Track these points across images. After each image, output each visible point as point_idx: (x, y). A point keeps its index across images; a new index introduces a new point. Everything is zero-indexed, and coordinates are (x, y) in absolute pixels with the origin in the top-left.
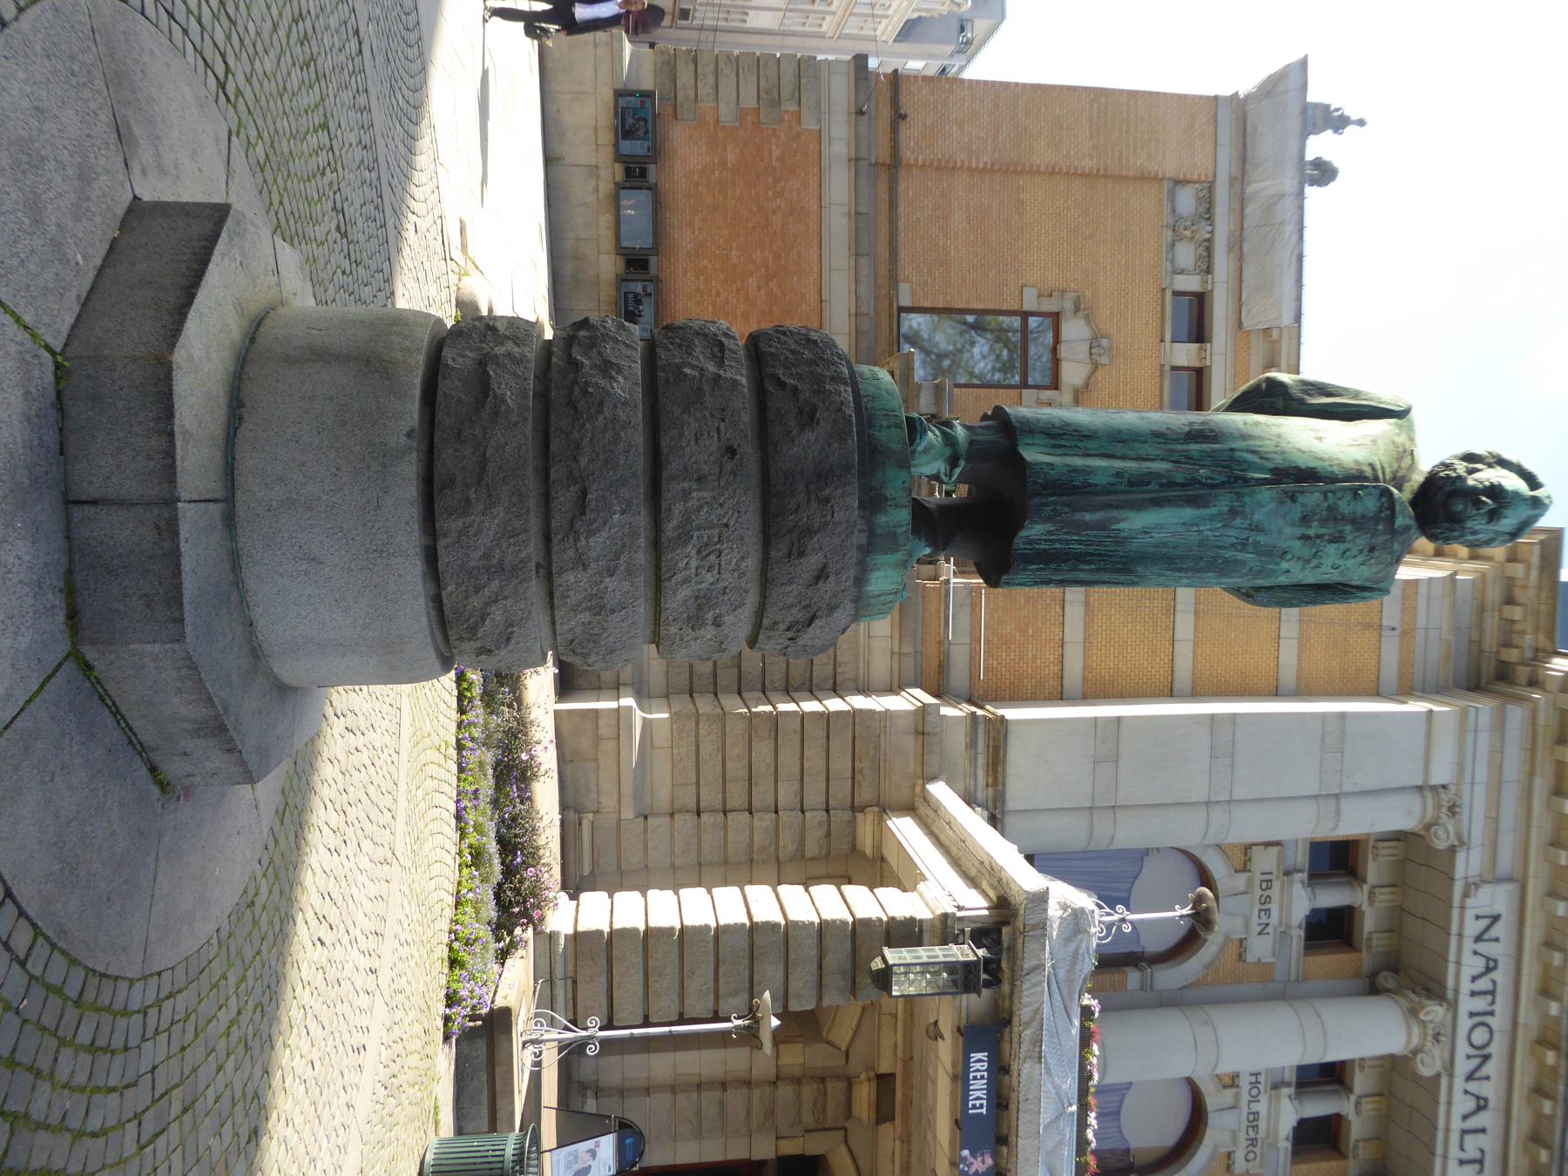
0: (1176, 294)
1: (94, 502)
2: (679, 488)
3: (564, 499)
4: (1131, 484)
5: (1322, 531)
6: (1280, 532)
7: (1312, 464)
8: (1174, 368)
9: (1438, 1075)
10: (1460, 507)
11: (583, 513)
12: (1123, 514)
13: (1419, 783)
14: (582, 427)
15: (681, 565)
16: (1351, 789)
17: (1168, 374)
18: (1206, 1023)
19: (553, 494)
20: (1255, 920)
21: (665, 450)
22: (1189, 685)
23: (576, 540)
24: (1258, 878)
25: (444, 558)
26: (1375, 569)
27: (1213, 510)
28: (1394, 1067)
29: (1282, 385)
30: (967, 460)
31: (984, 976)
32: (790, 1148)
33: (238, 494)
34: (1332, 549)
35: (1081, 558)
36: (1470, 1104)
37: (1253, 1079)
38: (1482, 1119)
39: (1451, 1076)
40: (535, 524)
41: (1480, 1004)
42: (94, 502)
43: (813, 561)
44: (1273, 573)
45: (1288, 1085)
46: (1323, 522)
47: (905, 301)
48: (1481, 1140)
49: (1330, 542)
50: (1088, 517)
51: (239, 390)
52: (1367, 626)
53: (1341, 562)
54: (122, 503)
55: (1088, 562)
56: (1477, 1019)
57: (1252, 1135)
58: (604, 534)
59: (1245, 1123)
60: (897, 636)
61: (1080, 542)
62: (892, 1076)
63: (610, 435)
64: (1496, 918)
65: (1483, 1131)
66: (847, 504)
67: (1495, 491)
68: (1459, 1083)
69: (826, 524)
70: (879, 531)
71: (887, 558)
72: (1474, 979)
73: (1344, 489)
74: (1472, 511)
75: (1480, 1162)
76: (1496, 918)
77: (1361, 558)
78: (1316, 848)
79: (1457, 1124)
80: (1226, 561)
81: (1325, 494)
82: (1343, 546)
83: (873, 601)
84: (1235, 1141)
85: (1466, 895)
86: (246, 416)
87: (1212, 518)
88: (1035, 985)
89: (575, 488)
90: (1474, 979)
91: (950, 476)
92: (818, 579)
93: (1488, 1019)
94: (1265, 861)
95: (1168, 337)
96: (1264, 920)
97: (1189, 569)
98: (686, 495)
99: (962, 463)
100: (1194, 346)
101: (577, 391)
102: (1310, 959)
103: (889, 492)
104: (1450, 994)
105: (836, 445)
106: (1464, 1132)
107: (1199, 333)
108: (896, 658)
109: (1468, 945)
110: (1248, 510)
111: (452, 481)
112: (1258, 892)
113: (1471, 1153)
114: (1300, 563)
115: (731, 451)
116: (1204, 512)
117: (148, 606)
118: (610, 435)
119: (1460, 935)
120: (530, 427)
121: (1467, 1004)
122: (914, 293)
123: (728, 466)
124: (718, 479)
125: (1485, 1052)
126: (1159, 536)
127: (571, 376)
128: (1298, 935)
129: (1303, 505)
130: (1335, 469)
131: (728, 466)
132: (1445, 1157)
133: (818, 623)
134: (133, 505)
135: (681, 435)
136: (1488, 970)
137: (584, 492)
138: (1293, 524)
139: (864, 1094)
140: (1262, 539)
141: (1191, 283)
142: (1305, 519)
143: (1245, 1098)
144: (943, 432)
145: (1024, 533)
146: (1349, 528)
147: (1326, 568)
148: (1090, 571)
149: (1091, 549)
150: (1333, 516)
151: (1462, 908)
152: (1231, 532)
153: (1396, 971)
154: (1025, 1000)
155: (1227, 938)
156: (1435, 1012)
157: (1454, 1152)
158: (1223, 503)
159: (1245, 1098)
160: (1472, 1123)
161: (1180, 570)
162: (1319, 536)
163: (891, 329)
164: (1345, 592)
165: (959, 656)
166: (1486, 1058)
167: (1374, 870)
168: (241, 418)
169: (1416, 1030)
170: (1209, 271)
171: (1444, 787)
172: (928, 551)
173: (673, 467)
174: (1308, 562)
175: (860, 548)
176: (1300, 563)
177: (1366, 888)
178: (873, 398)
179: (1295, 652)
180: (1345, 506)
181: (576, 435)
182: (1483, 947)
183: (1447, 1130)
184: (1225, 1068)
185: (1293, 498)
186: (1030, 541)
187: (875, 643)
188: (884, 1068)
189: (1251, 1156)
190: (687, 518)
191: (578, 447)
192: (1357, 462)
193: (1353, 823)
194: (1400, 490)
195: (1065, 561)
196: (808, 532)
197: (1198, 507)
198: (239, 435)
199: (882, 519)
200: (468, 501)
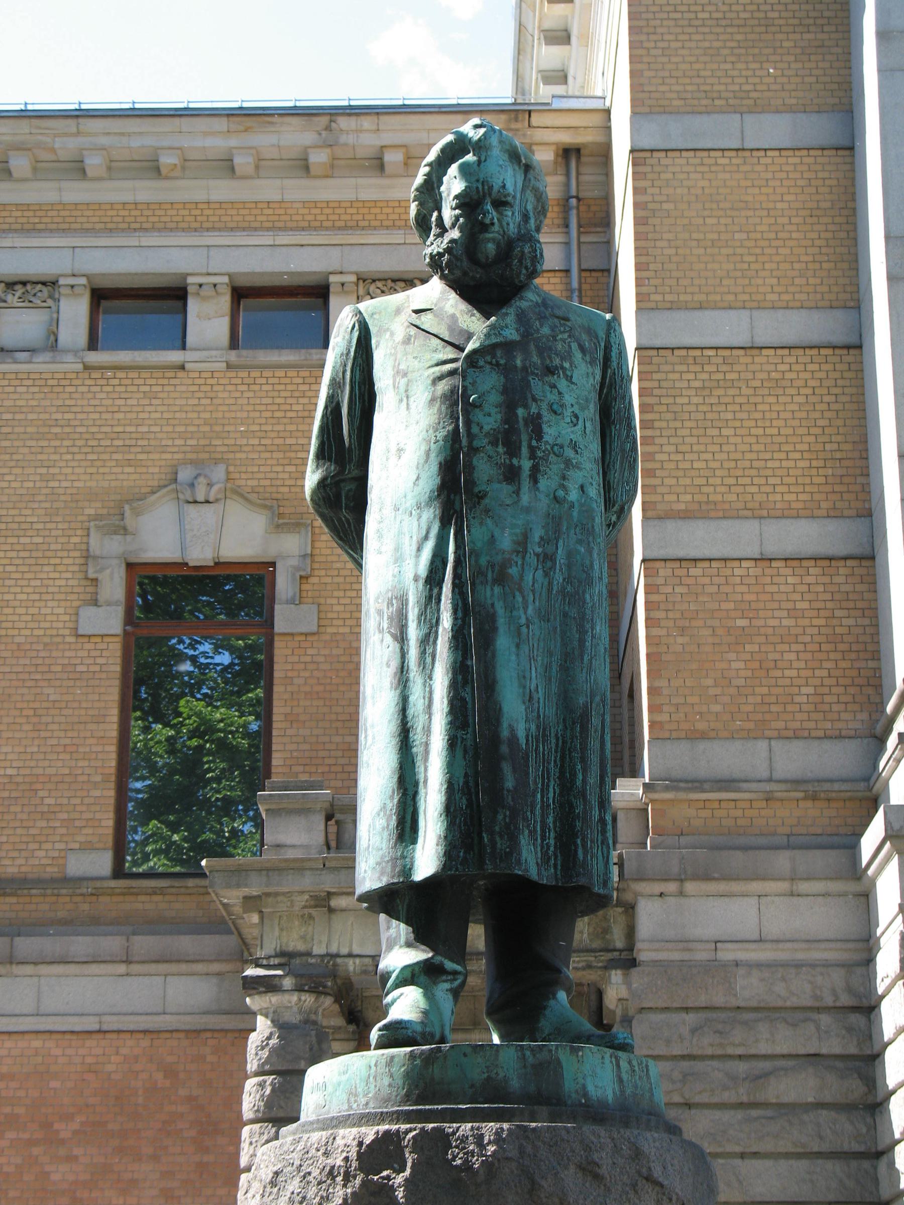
0: (93, 344)
5: (525, 451)
6: (527, 510)
7: (434, 468)
8: (234, 343)
10: (491, 247)
17: (245, 355)
22: (839, 314)
26: (578, 355)
29: (322, 484)
34: (550, 433)
35: (567, 785)
44: (588, 512)
46: (513, 450)
47: (103, 863)
49: (539, 438)
53: (568, 413)
55: (574, 775)
60: (756, 886)
61: (545, 790)
67: (468, 203)
70: (532, 1088)
73: (468, 423)
74: (494, 233)
77: (562, 384)
80: (568, 580)
82: (546, 415)
83: (628, 1091)
87: (510, 608)
91: (455, 973)
92: (597, 1177)
95: (175, 356)
97: (582, 632)
100: (193, 306)
107: (169, 297)
108: (804, 887)
114: (570, 473)
116: (501, 622)
122: (87, 847)
126: (535, 680)
130: (441, 434)
133: (657, 1173)
138: (517, 492)
140: (537, 534)
141: (75, 313)
142: (511, 475)
144: (397, 986)
145: (533, 873)
146: (521, 412)
147: (576, 436)
148: (585, 771)
149: (554, 771)
150: (508, 438)
152: (529, 578)
161: (582, 642)
162: (532, 456)
163: (154, 892)
164: (612, 385)
165: (796, 759)
170: (51, 284)
172: (562, 995)
174: (568, 463)
176: (570, 473)
178: (353, 1093)
179: (768, 119)
180: (490, 420)
185: (481, 496)
186: (545, 859)
187: (773, 929)
192: (432, 400)
194: (469, 336)
195: (571, 807)
197: (495, 629)
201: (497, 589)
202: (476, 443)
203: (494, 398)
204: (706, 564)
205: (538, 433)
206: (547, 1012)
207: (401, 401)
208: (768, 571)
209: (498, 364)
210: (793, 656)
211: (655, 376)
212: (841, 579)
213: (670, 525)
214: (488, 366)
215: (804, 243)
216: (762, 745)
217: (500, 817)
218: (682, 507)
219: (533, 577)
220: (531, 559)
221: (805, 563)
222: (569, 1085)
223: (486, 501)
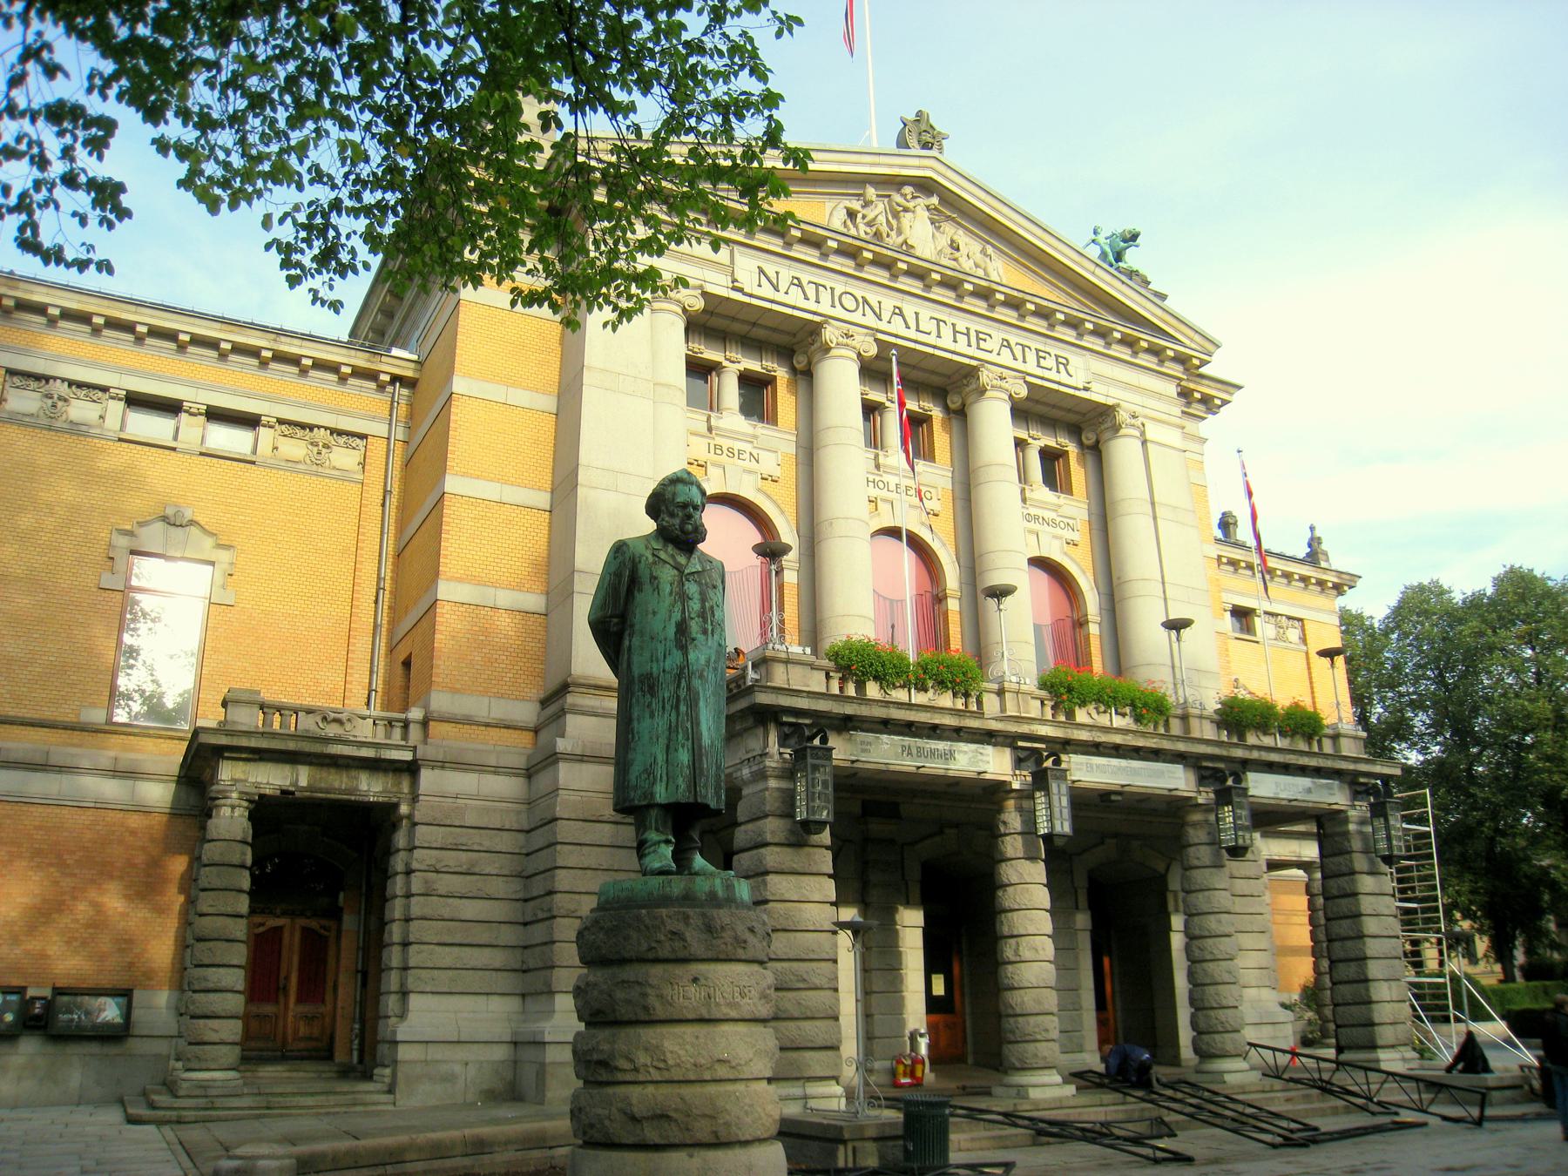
3: (722, 1072)
9: (876, 340)
20: (746, 464)
28: (873, 371)
31: (817, 742)
36: (898, 319)
39: (878, 331)
41: (825, 296)
45: (877, 456)
46: (705, 621)
64: (761, 271)
68: (882, 326)
72: (807, 298)
76: (761, 271)
78: (692, 401)
79: (912, 334)
85: (741, 290)
89: (717, 1066)
90: (807, 298)
93: (837, 294)
96: (747, 456)
98: (717, 1004)
103: (707, 889)
109: (779, 297)
113: (932, 327)
121: (825, 308)
128: (762, 430)
131: (703, 981)
136: (800, 285)
139: (877, 827)
142: (705, 632)
143: (884, 494)
150: (702, 615)
151: (751, 296)
155: (759, 490)
157: (931, 340)
158: (696, 683)
159: (884, 494)
160: (912, 324)
166: (865, 301)
167: (711, 354)
169: (843, 352)
170: (104, 389)
177: (725, 363)
182: (783, 288)
183: (916, 342)
190: (730, 1005)
193: (677, 372)
196: (736, 938)
203: (697, 596)
205: (713, 615)
213: (452, 584)
216: (486, 700)
219: (711, 676)
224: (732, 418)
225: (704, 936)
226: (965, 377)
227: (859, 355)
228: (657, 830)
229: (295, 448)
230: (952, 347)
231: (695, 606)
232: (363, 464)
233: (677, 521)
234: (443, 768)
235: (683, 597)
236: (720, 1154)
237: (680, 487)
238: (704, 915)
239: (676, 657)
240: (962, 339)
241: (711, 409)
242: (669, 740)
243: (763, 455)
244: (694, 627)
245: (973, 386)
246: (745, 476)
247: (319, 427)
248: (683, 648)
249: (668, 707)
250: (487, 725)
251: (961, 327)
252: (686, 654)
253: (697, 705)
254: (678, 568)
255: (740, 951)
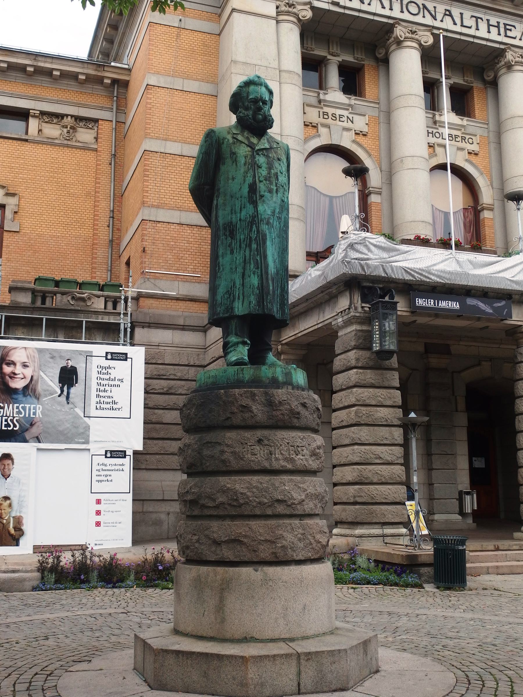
1: (299, 684)
2: (274, 462)
3: (280, 509)
4: (258, 268)
5: (274, 184)
6: (275, 203)
9: (433, 34)
11: (285, 501)
12: (270, 272)
13: (275, 21)
14: (250, 501)
15: (302, 462)
16: (277, 62)
18: (402, 161)
19: (277, 513)
20: (345, 124)
21: (259, 467)
23: (294, 504)
24: (321, 120)
25: (300, 557)
27: (268, 234)
28: (429, 57)
30: (244, 338)
31: (387, 299)
32: (462, 404)
33: (282, 637)
36: (448, 19)
37: (430, 135)
38: (456, 12)
39: (434, 27)
40: (287, 521)
42: (299, 684)
43: (300, 409)
45: (434, 115)
46: (271, 183)
48: (467, 14)
50: (271, 288)
51: (239, 640)
52: (178, 36)
54: (299, 673)
56: (405, 9)
57: (459, 139)
58: (293, 493)
59: (453, 142)
62: (425, 344)
63: (254, 490)
65: (461, 14)
66: (280, 394)
68: (437, 24)
69: (288, 403)
71: (294, 377)
72: (383, 7)
75: (477, 18)
77: (282, 164)
79: (458, 28)
80: (284, 226)
81: (260, 181)
82: (279, 174)
84: (462, 149)
86: (250, 636)
88: (393, 270)
94: (313, 115)
96: (345, 119)
98: (277, 459)
99: (246, 339)
101: (235, 504)
102: (368, 93)
103: (270, 375)
104: (391, 21)
105: (257, 398)
106: (462, 25)
110: (267, 217)
111: (273, 553)
112: (329, 121)
113: (472, 22)
115: (260, 441)
116: (268, 237)
117: (334, 663)
118: (254, 490)
119: (359, 11)
120: (251, 523)
121: (396, 13)
123: (266, 442)
124: (271, 446)
125: (421, 7)
126: (276, 256)
127: (227, 506)
128: (353, 100)
129: (264, 192)
132: (474, 37)
134: (299, 670)
135: (253, 461)
137: (278, 501)
138: (272, 196)
139: (434, 361)
140: (277, 210)
151: (345, 8)
152: (275, 224)
153: (376, 46)
154: (401, 277)
155: (354, 141)
156: (399, 32)
157: (472, 32)
158: (264, 227)
159: (440, 141)
160: (458, 21)
162: (276, 186)
166: (424, 7)
167: (320, 52)
168: (252, 638)
171: (277, 7)
173: (267, 465)
175: (293, 389)
177: (329, 57)
179: (191, 82)
181: (255, 504)
184: (424, 151)
188: (421, 348)
189: (470, 141)
190: (286, 459)
191: (260, 503)
198: (258, 638)
199: (280, 379)
200: (282, 547)
201: (267, 227)
202: (261, 179)
203: (264, 166)
204: (162, 223)
205: (277, 179)
206: (268, 358)
207: (233, 162)
208: (181, 228)
209: (264, 155)
210: (187, 256)
211: (150, 160)
212: (204, 233)
214: (262, 155)
215: (200, 124)
217: (269, 297)
218: (156, 204)
219: (276, 224)
220: (275, 218)
221: (193, 227)
222: (294, 380)
223: (264, 198)
224: (335, 95)
225: (266, 409)
226: (496, 57)
227: (420, 45)
228: (236, 335)
229: (52, 131)
230: (486, 35)
231: (264, 172)
232: (96, 138)
233: (250, 113)
234: (149, 327)
235: (254, 166)
236: (278, 570)
237: (252, 88)
238: (266, 394)
239: (250, 209)
240: (494, 30)
241: (321, 88)
242: (244, 269)
243: (356, 118)
244: (262, 187)
245: (503, 63)
246: (345, 133)
247: (67, 115)
248: (255, 204)
249: (243, 246)
250: (177, 299)
251: (493, 21)
252: (256, 207)
253: (264, 242)
254: (251, 146)
255: (295, 420)
